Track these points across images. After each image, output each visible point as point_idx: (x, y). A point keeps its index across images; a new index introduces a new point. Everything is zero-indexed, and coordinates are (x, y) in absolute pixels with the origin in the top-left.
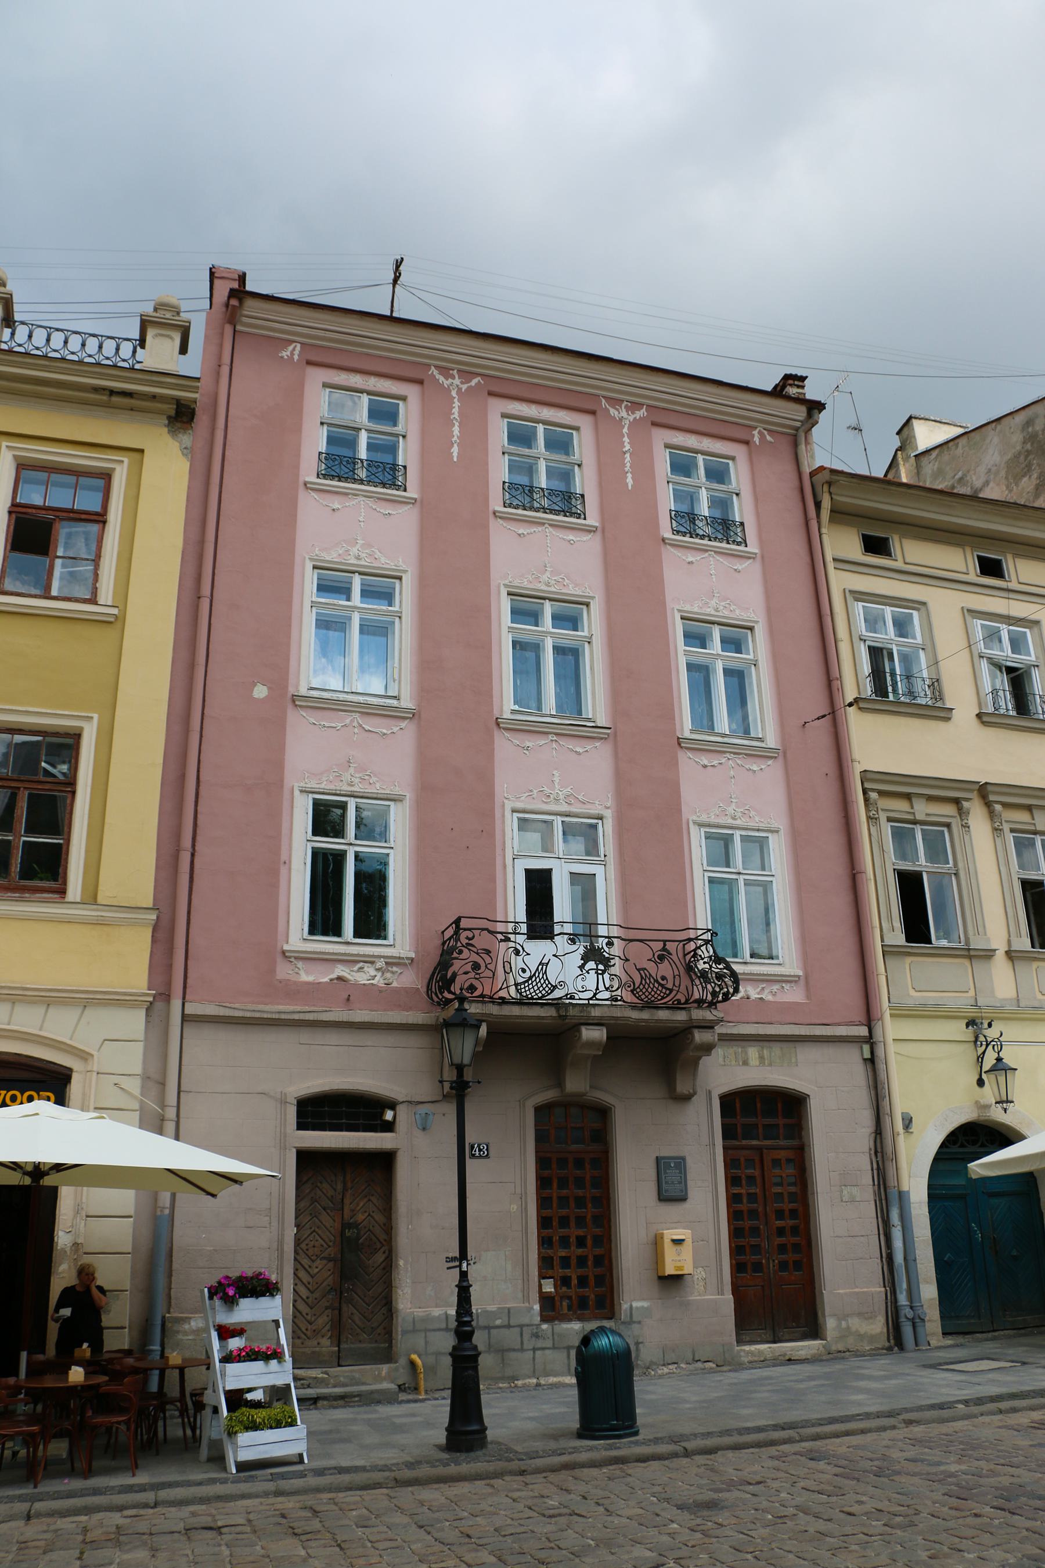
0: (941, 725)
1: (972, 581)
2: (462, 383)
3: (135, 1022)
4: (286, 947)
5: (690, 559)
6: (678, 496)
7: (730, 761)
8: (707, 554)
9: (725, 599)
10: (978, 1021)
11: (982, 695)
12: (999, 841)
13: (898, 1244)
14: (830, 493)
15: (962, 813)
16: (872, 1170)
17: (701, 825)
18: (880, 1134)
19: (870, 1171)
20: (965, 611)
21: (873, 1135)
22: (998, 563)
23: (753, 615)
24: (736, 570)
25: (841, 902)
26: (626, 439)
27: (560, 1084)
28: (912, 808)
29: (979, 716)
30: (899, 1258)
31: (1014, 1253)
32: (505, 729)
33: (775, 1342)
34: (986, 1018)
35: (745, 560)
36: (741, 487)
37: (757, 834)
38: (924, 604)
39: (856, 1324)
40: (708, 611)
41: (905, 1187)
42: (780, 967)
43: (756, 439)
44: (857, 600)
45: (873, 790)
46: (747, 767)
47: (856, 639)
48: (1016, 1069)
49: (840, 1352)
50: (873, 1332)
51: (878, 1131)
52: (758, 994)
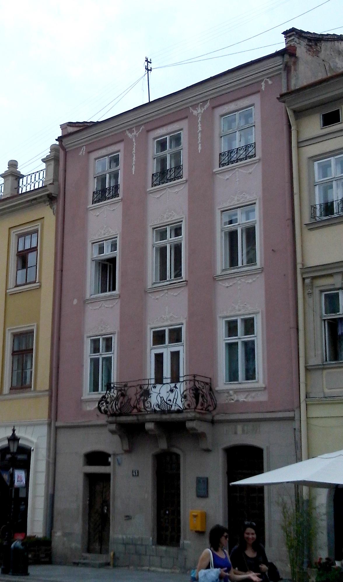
2: (137, 133)
3: (44, 430)
4: (82, 398)
5: (227, 177)
8: (234, 171)
17: (224, 317)
26: (200, 125)
27: (158, 447)
32: (150, 293)
43: (263, 88)
45: (308, 278)
46: (247, 281)
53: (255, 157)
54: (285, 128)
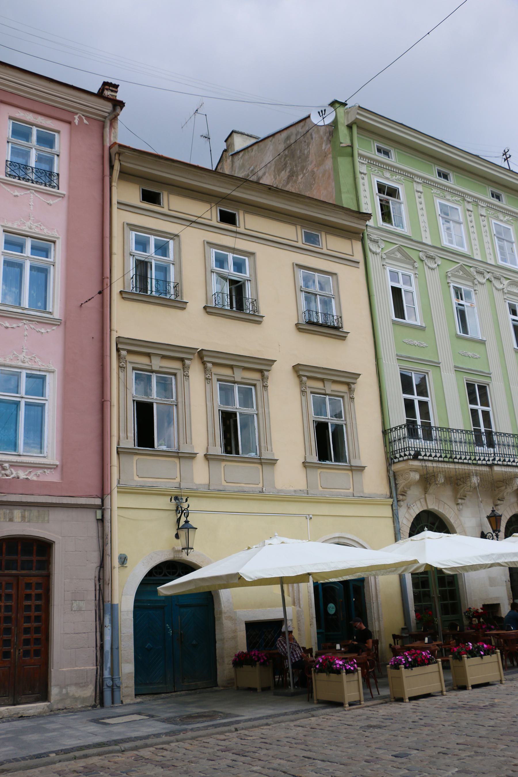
0: (179, 312)
1: (215, 226)
5: (16, 193)
6: (15, 152)
7: (26, 326)
8: (29, 192)
9: (38, 222)
10: (180, 497)
11: (209, 295)
12: (208, 386)
13: (107, 638)
14: (120, 160)
15: (185, 368)
16: (95, 590)
18: (103, 567)
19: (94, 592)
20: (205, 243)
21: (99, 568)
22: (234, 215)
24: (48, 204)
25: (92, 420)
28: (151, 362)
29: (205, 308)
30: (107, 647)
31: (194, 642)
33: (14, 705)
34: (184, 496)
36: (61, 151)
37: (38, 373)
39: (73, 691)
40: (24, 228)
41: (116, 601)
42: (44, 458)
43: (76, 121)
44: (132, 230)
46: (37, 330)
47: (127, 254)
48: (196, 528)
49: (59, 709)
50: (85, 696)
51: (102, 566)
52: (27, 475)
54: (107, 179)
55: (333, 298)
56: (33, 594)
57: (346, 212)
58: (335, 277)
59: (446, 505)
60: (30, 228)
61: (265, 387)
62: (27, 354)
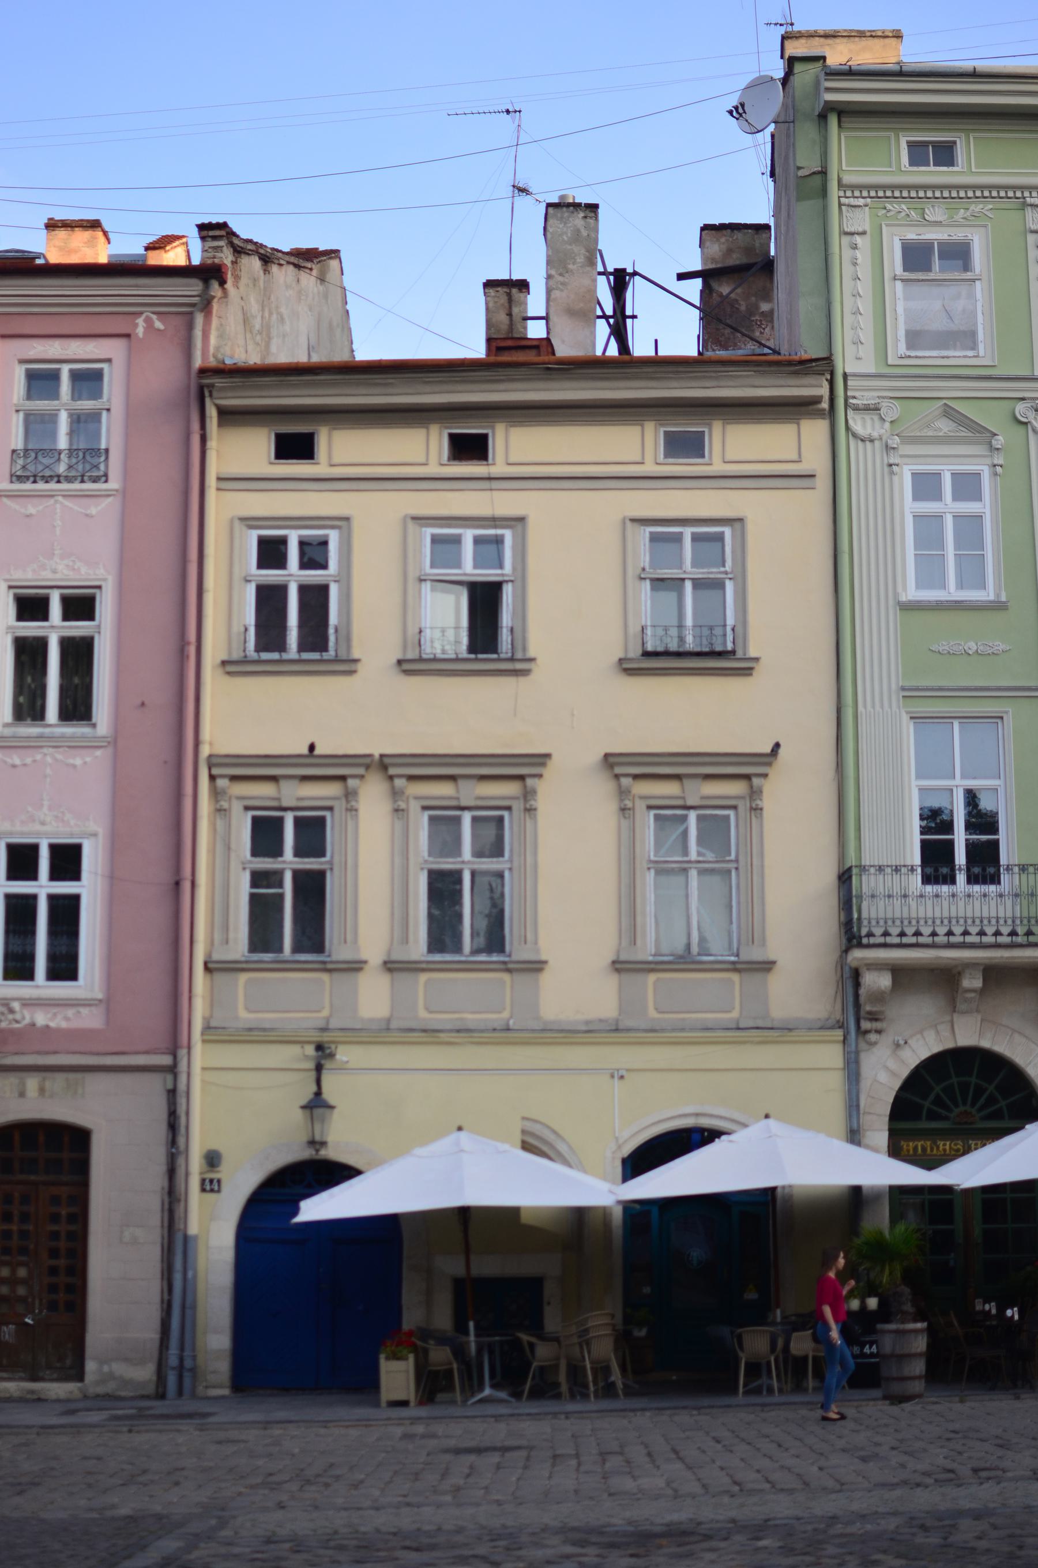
5: (31, 510)
8: (52, 501)
12: (398, 825)
15: (350, 795)
23: (102, 571)
29: (400, 662)
35: (102, 499)
38: (347, 519)
39: (119, 1369)
41: (193, 1229)
43: (140, 331)
45: (222, 776)
51: (171, 1172)
52: (51, 1019)
53: (106, 481)
55: (730, 579)
56: (64, 1213)
57: (756, 369)
58: (738, 525)
59: (1016, 1036)
60: (54, 572)
61: (530, 810)
62: (50, 809)
